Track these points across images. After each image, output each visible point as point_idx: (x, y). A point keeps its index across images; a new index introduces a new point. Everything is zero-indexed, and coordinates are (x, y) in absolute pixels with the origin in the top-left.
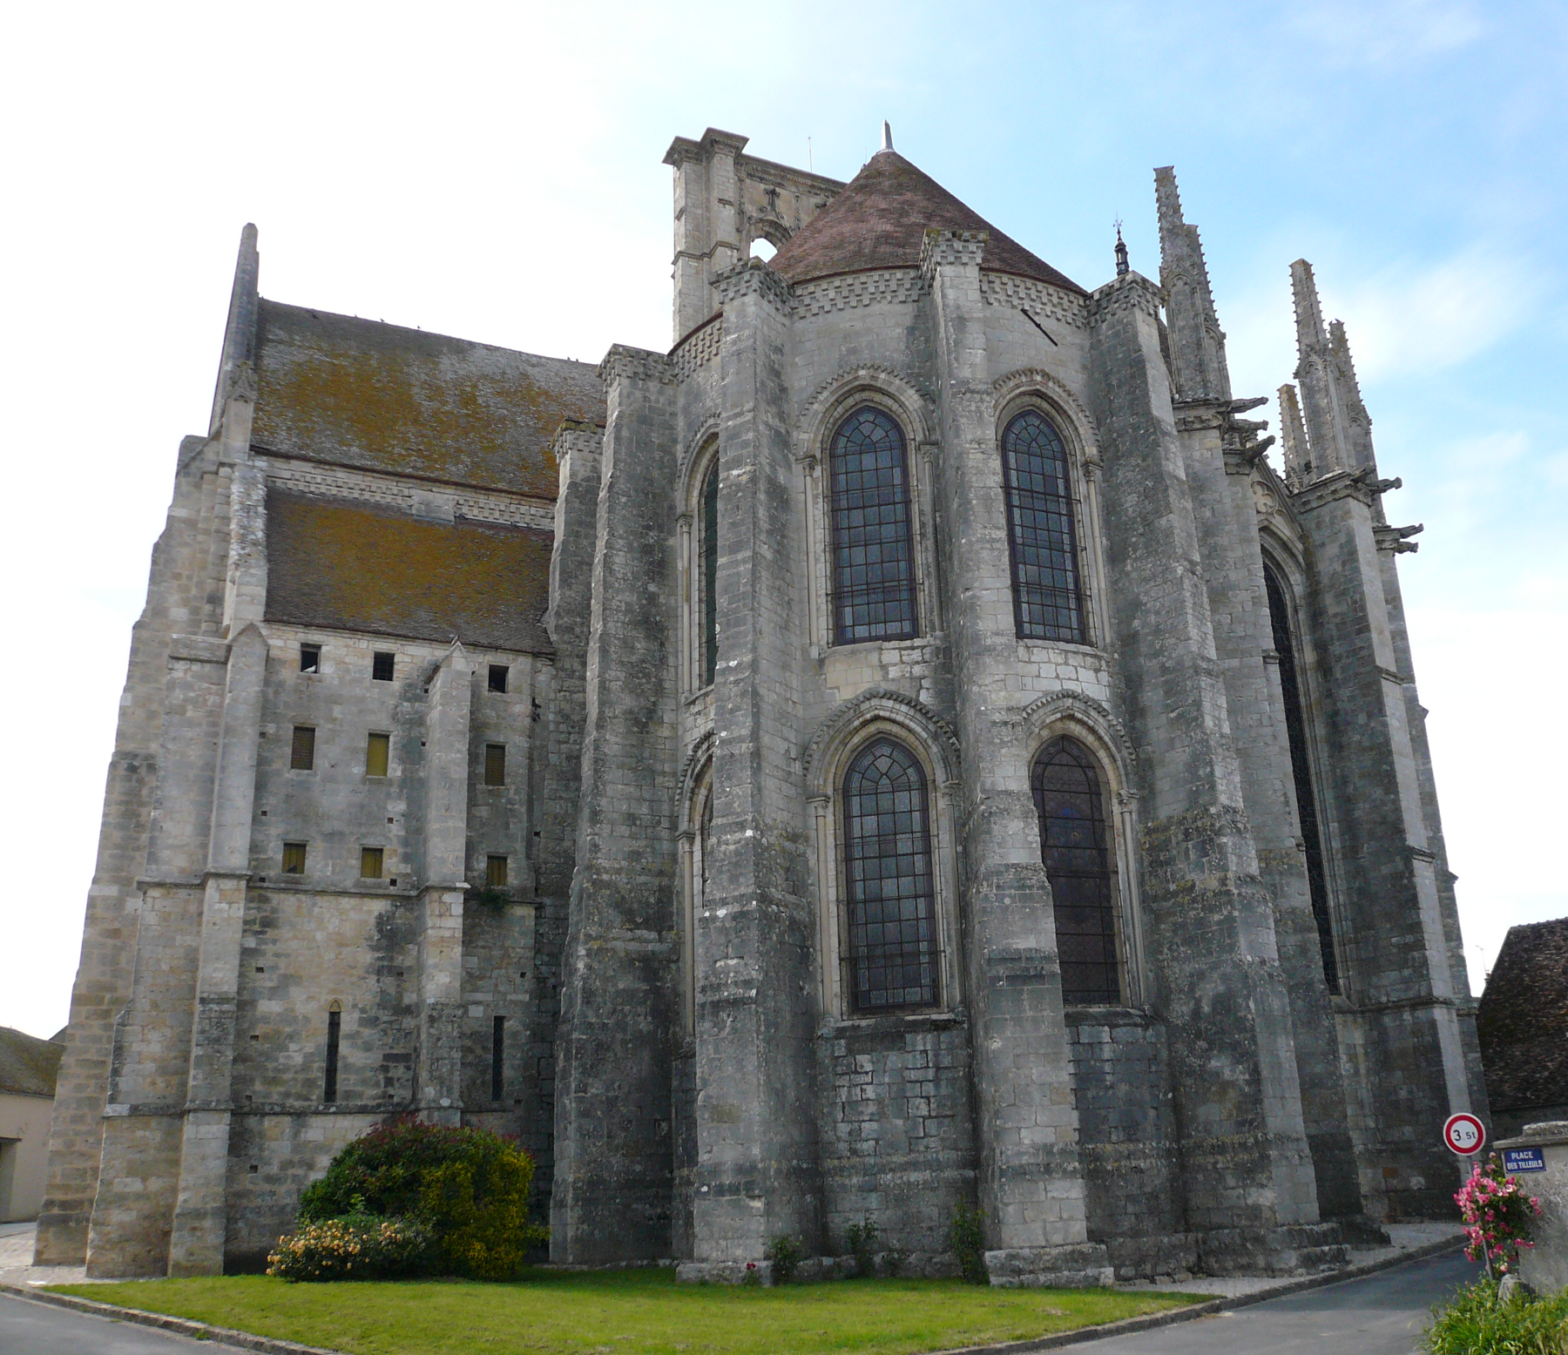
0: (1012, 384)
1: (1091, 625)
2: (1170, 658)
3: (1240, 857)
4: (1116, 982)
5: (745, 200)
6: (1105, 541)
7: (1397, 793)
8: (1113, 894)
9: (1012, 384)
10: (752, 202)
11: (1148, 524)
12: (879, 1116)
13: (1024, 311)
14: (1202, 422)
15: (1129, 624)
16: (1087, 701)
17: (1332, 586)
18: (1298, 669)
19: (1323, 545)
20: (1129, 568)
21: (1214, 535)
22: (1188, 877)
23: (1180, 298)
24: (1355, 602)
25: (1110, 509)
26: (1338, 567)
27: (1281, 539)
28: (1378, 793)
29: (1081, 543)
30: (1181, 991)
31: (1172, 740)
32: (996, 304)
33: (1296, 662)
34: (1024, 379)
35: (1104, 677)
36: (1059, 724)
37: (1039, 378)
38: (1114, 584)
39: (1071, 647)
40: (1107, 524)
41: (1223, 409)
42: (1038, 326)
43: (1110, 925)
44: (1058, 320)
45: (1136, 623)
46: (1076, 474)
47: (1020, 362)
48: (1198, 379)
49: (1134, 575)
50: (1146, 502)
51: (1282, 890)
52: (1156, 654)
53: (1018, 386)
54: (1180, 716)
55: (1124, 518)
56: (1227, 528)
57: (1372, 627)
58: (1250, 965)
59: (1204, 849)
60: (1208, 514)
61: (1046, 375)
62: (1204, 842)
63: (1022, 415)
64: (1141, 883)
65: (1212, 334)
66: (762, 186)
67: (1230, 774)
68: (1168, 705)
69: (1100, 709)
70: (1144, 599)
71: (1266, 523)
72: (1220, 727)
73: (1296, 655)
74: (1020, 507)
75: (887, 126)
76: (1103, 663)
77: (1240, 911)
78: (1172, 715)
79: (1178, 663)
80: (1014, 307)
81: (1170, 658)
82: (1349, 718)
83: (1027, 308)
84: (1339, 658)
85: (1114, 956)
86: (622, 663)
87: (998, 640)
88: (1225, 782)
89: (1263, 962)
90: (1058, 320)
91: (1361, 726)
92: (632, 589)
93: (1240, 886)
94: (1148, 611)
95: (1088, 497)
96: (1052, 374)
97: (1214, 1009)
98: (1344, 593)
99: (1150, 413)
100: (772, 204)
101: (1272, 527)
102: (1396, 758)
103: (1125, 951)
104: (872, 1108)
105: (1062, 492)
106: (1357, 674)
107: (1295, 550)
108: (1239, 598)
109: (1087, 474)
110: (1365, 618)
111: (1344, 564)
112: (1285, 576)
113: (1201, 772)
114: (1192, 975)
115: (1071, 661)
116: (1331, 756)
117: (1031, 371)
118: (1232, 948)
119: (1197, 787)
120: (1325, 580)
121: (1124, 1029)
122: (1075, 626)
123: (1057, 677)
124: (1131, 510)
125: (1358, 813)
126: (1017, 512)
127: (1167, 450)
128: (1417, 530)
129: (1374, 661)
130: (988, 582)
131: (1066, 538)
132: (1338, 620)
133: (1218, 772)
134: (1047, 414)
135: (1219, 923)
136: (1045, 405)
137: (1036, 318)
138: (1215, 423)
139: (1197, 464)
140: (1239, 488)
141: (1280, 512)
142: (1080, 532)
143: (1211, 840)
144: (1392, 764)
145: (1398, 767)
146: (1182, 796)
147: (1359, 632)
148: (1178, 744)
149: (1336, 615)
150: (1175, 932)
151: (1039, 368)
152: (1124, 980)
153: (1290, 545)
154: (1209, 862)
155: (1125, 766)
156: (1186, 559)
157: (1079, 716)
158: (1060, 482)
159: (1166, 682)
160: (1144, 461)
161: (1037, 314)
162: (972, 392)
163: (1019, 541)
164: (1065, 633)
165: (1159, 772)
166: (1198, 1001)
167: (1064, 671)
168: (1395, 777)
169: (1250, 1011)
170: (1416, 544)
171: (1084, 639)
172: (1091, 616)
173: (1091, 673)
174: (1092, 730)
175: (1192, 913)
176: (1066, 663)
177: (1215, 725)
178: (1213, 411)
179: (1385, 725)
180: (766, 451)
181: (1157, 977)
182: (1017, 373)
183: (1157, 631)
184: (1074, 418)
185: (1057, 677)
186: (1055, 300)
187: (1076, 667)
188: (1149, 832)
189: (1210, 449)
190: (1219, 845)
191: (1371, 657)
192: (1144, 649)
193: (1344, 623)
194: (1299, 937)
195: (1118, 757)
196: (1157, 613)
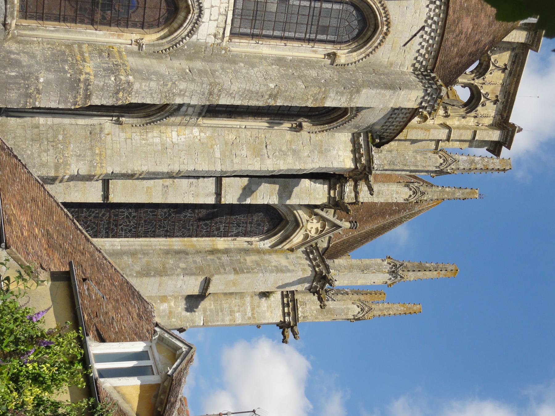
0: (381, 9)
1: (242, 41)
2: (221, 74)
3: (102, 89)
4: (31, 18)
6: (290, 58)
7: (136, 277)
8: (84, 25)
11: (299, 77)
13: (423, 28)
14: (360, 158)
15: (241, 62)
16: (197, 23)
17: (263, 260)
18: (214, 238)
19: (287, 258)
20: (274, 67)
21: (293, 155)
22: (91, 62)
23: (434, 159)
24: (252, 269)
25: (309, 64)
26: (274, 264)
27: (291, 235)
28: (137, 268)
29: (289, 43)
30: (24, 49)
31: (173, 68)
33: (219, 238)
34: (385, 19)
35: (211, 40)
36: (184, 5)
38: (263, 58)
39: (229, 21)
40: (301, 61)
41: (367, 169)
42: (415, 35)
43: (65, 20)
45: (242, 65)
46: (330, 48)
47: (392, 17)
48: (386, 162)
49: (270, 68)
50: (312, 79)
51: (82, 160)
52: (223, 69)
53: (380, 14)
54: (186, 73)
55: (303, 69)
56: (297, 163)
57: (237, 277)
58: (37, 79)
59: (108, 70)
61: (386, 34)
62: (112, 70)
64: (90, 44)
65: (413, 196)
67: (151, 94)
68: (193, 69)
69: (191, 32)
70: (256, 69)
72: (179, 95)
73: (222, 239)
74: (310, 7)
76: (219, 41)
77: (70, 79)
78: (188, 71)
79: (217, 76)
80: (426, 21)
81: (221, 74)
82: (183, 259)
83: (427, 29)
84: (220, 259)
85: (47, 20)
88: (147, 89)
89: (39, 92)
91: (178, 264)
93: (85, 84)
94: (248, 70)
95: (315, 52)
96: (388, 38)
97: (12, 59)
98: (258, 265)
99: (363, 87)
102: (157, 279)
103: (50, 25)
106: (209, 266)
108: (256, 163)
110: (242, 272)
111: (276, 267)
113: (153, 76)
114: (33, 53)
115: (221, 17)
116: (160, 249)
117: (388, 24)
118: (48, 70)
119: (145, 74)
120: (266, 257)
121: (3, 8)
122: (241, 31)
123: (212, 7)
124: (308, 72)
125: (125, 258)
127: (342, 94)
128: (295, 334)
129: (217, 274)
131: (292, 35)
132: (242, 260)
133: (153, 84)
134: (365, 35)
135: (64, 68)
136: (369, 33)
139: (335, 152)
141: (306, 236)
142: (296, 44)
143: (113, 73)
144: (154, 276)
145: (152, 280)
146: (140, 67)
147: (235, 270)
148: (169, 70)
149: (245, 260)
150: (60, 51)
151: (390, 29)
152: (33, 23)
153: (288, 241)
154: (100, 71)
155: (159, 45)
156: (278, 92)
157: (189, 18)
158: (323, 37)
159: (207, 71)
160: (336, 81)
164: (237, 24)
165: (154, 61)
166: (18, 54)
167: (215, 11)
168: (146, 276)
169: (9, 72)
170: (286, 342)
171: (233, 34)
172: (247, 41)
173: (213, 31)
174: (181, 25)
175: (70, 59)
176: (220, 14)
177: (181, 91)
179: (178, 275)
181: (35, 41)
183: (236, 71)
184: (362, 50)
185: (212, 7)
187: (217, 20)
188: (119, 52)
189: (344, 161)
190: (109, 76)
191: (220, 273)
192: (226, 65)
193: (240, 263)
194: (52, 165)
195: (164, 41)
196: (247, 73)
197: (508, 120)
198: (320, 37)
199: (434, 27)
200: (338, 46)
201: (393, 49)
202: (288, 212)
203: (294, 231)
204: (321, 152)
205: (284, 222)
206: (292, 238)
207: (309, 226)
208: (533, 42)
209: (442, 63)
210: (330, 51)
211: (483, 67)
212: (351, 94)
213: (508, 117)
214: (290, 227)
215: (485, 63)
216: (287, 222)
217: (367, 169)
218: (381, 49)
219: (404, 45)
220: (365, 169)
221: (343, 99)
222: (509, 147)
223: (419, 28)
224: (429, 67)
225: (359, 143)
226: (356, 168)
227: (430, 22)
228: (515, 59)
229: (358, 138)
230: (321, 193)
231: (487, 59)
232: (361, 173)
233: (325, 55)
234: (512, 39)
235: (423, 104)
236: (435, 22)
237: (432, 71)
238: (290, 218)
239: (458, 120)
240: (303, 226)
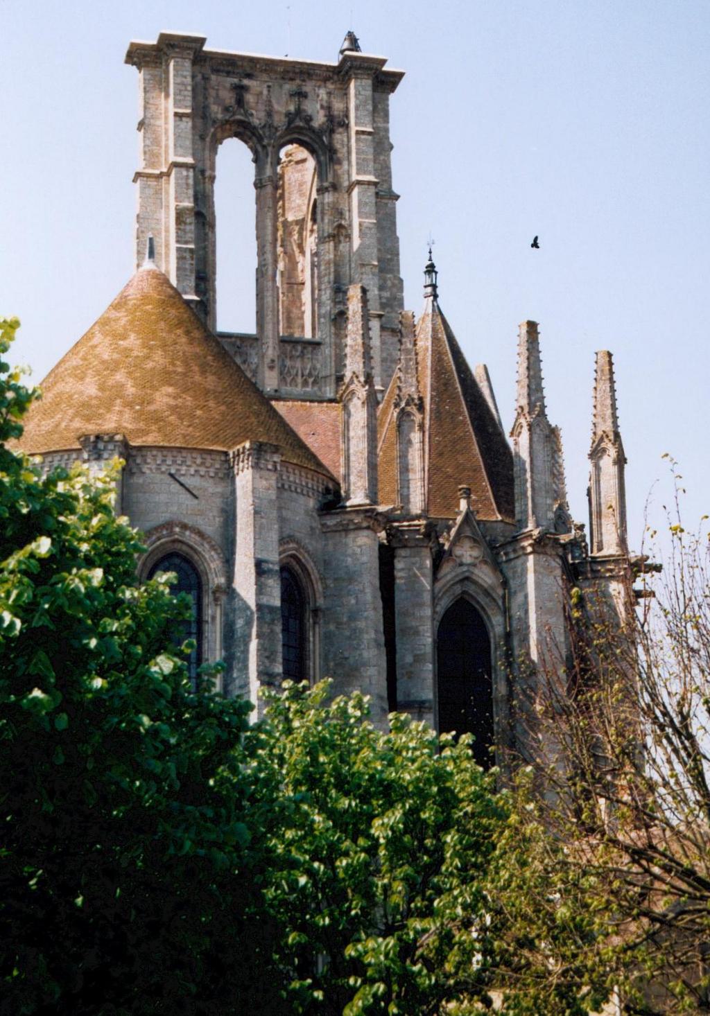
9: (154, 538)
13: (171, 475)
32: (148, 472)
34: (165, 532)
37: (177, 529)
41: (369, 514)
42: (182, 485)
44: (202, 476)
46: (208, 599)
53: (159, 539)
56: (366, 614)
60: (353, 601)
61: (185, 527)
71: (467, 574)
80: (163, 473)
83: (173, 471)
90: (202, 476)
95: (214, 618)
96: (190, 524)
101: (474, 577)
107: (494, 595)
108: (369, 673)
109: (216, 600)
112: (489, 617)
117: (169, 525)
137: (182, 479)
138: (365, 524)
140: (417, 559)
142: (205, 646)
153: (491, 592)
161: (183, 475)
178: (362, 516)
182: (156, 529)
186: (199, 461)
189: (360, 547)
197: (334, 67)
199: (169, 462)
200: (205, 588)
201: (201, 513)
202: (448, 594)
203: (475, 583)
205: (466, 597)
206: (486, 585)
208: (190, 49)
209: (216, 439)
210: (211, 598)
211: (241, 130)
213: (328, 68)
214: (472, 589)
215: (234, 128)
216: (464, 592)
217: (369, 514)
218: (203, 528)
219: (196, 497)
220: (370, 517)
222: (383, 62)
223: (173, 482)
224: (223, 458)
225: (335, 525)
226: (368, 528)
227: (163, 469)
228: (222, 71)
229: (328, 527)
230: (413, 560)
231: (228, 126)
232: (376, 520)
233: (216, 605)
234: (186, 90)
235: (270, 467)
236: (164, 461)
237: (226, 454)
238: (458, 590)
239: (339, 162)
240: (468, 571)
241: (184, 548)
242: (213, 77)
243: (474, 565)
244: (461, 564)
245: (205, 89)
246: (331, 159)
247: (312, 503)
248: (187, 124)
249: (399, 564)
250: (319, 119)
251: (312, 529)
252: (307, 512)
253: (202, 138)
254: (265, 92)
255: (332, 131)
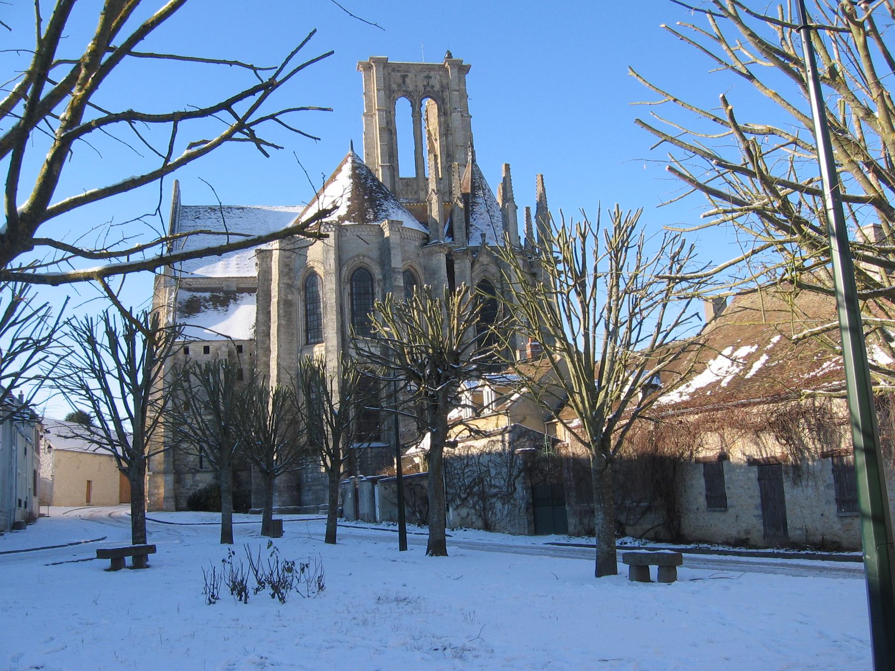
5: (392, 83)
10: (395, 83)
12: (312, 473)
46: (376, 285)
61: (364, 256)
63: (359, 269)
66: (399, 74)
75: (352, 142)
86: (262, 348)
87: (332, 348)
92: (264, 325)
95: (378, 292)
100: (404, 82)
104: (310, 471)
105: (370, 291)
109: (379, 285)
117: (358, 256)
126: (354, 301)
130: (330, 332)
137: (362, 237)
162: (330, 274)
163: (355, 310)
180: (283, 292)
182: (352, 258)
189: (438, 260)
198: (370, 291)
203: (489, 272)
204: (434, 274)
207: (485, 263)
212: (395, 272)
214: (487, 274)
221: (399, 276)
230: (461, 264)
239: (446, 104)
241: (365, 265)
242: (392, 73)
243: (487, 264)
244: (483, 265)
245: (390, 78)
246: (443, 103)
247: (417, 244)
248: (382, 93)
249: (456, 266)
250: (437, 87)
251: (418, 254)
252: (415, 247)
253: (389, 98)
254: (414, 77)
255: (442, 91)
